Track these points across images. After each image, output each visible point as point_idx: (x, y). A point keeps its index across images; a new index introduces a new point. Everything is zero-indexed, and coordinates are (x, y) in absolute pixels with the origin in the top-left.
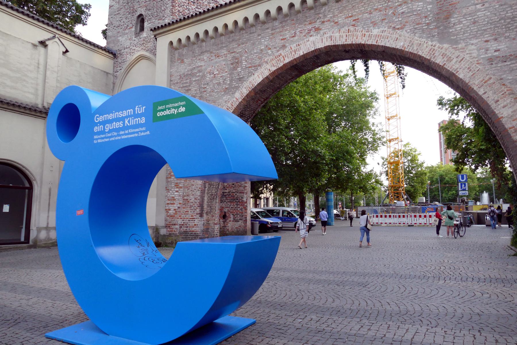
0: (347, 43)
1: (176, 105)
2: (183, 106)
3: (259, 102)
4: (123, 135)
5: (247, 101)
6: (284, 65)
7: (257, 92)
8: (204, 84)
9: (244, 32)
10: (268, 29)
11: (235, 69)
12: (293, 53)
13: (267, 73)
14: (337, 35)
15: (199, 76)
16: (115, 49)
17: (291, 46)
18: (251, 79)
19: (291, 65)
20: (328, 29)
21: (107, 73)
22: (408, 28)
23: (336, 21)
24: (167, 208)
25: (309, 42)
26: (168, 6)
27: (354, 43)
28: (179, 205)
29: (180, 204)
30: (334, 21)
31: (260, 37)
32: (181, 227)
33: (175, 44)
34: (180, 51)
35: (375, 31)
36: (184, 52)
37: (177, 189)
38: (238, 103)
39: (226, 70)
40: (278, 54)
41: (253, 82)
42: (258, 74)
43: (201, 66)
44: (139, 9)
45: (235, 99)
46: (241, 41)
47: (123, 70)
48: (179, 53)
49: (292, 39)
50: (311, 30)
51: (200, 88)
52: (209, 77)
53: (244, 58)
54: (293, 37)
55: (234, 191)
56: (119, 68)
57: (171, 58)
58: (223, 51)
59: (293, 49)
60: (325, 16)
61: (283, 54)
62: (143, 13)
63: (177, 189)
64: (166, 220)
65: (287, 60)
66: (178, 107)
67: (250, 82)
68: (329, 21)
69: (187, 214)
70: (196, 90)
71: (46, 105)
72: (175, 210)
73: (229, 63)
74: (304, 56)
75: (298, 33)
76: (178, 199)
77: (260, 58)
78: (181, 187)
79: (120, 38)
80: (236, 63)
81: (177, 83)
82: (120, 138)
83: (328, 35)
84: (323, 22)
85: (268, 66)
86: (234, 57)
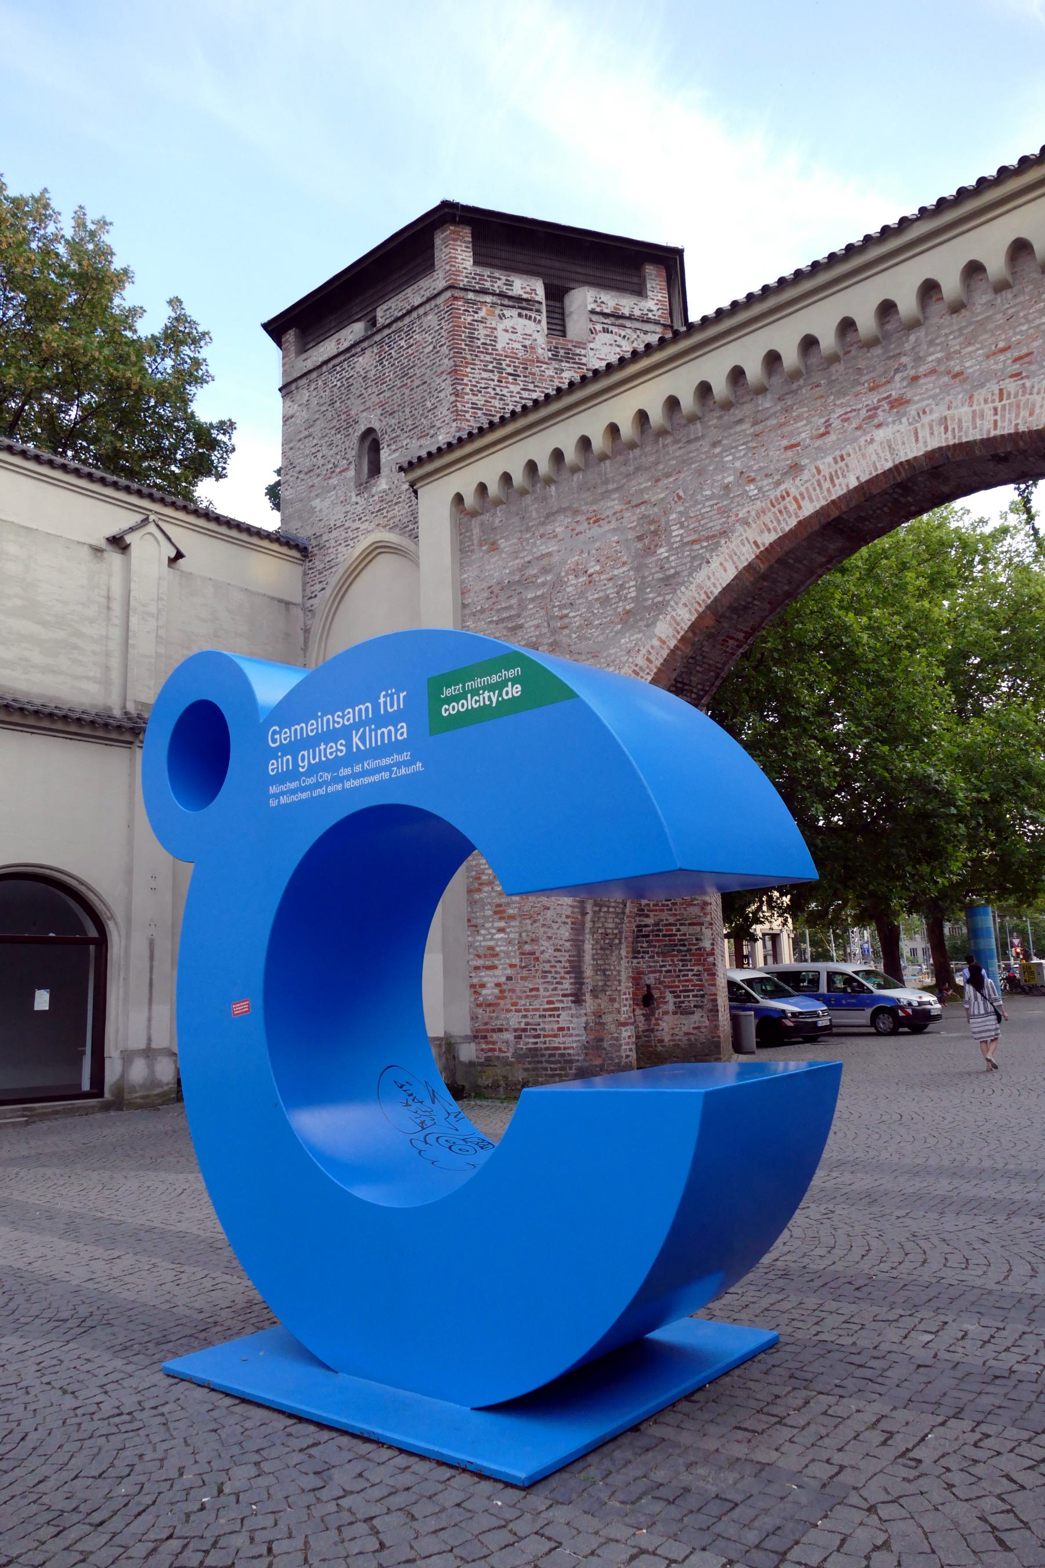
0: (998, 432)
1: (495, 679)
2: (515, 681)
3: (731, 642)
4: (348, 778)
5: (693, 644)
6: (800, 522)
7: (723, 616)
8: (561, 607)
9: (669, 440)
10: (740, 421)
11: (649, 551)
12: (827, 485)
13: (747, 555)
14: (964, 411)
15: (544, 584)
16: (303, 532)
17: (819, 463)
18: (700, 577)
19: (823, 521)
20: (934, 397)
21: (288, 604)
23: (957, 369)
24: (475, 981)
25: (871, 449)
26: (442, 395)
27: (1022, 428)
28: (509, 972)
29: (512, 966)
30: (948, 372)
31: (718, 450)
32: (519, 1037)
34: (486, 517)
36: (497, 520)
37: (502, 924)
38: (665, 653)
39: (625, 559)
40: (778, 493)
41: (709, 583)
42: (720, 559)
43: (549, 555)
44: (365, 414)
45: (656, 642)
46: (661, 467)
47: (328, 591)
48: (482, 524)
49: (818, 443)
50: (876, 408)
51: (550, 618)
52: (573, 584)
53: (674, 516)
54: (823, 435)
55: (672, 920)
56: (318, 587)
57: (461, 542)
58: (609, 504)
59: (825, 471)
60: (918, 360)
61: (794, 491)
62: (376, 425)
63: (502, 924)
64: (474, 1018)
65: (809, 509)
66: (500, 686)
67: (700, 587)
68: (933, 371)
69: (536, 997)
70: (537, 626)
71: (131, 708)
72: (498, 985)
73: (631, 535)
74: (861, 489)
75: (836, 423)
76: (507, 953)
77: (724, 512)
78: (512, 917)
79: (316, 503)
80: (652, 533)
81: (482, 611)
82: (339, 787)
83: (935, 416)
84: (915, 379)
85: (751, 534)
86: (644, 517)
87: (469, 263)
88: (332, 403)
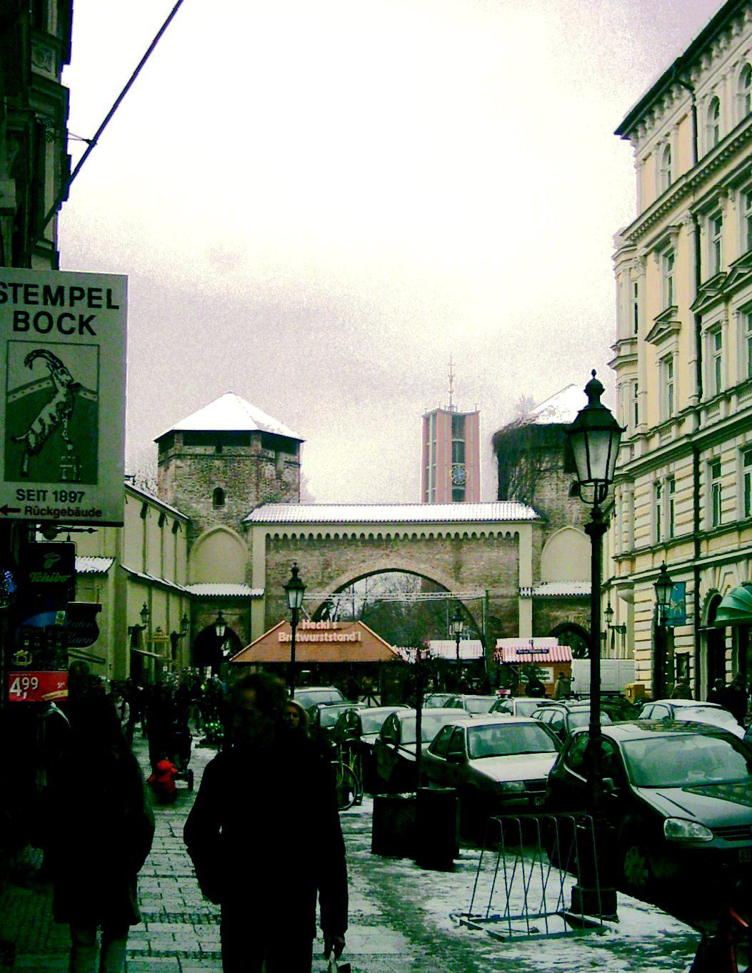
11: (326, 568)
18: (339, 579)
22: (440, 569)
33: (272, 536)
35: (422, 566)
47: (199, 538)
60: (392, 547)
77: (347, 566)
80: (327, 565)
87: (260, 447)
88: (202, 471)
